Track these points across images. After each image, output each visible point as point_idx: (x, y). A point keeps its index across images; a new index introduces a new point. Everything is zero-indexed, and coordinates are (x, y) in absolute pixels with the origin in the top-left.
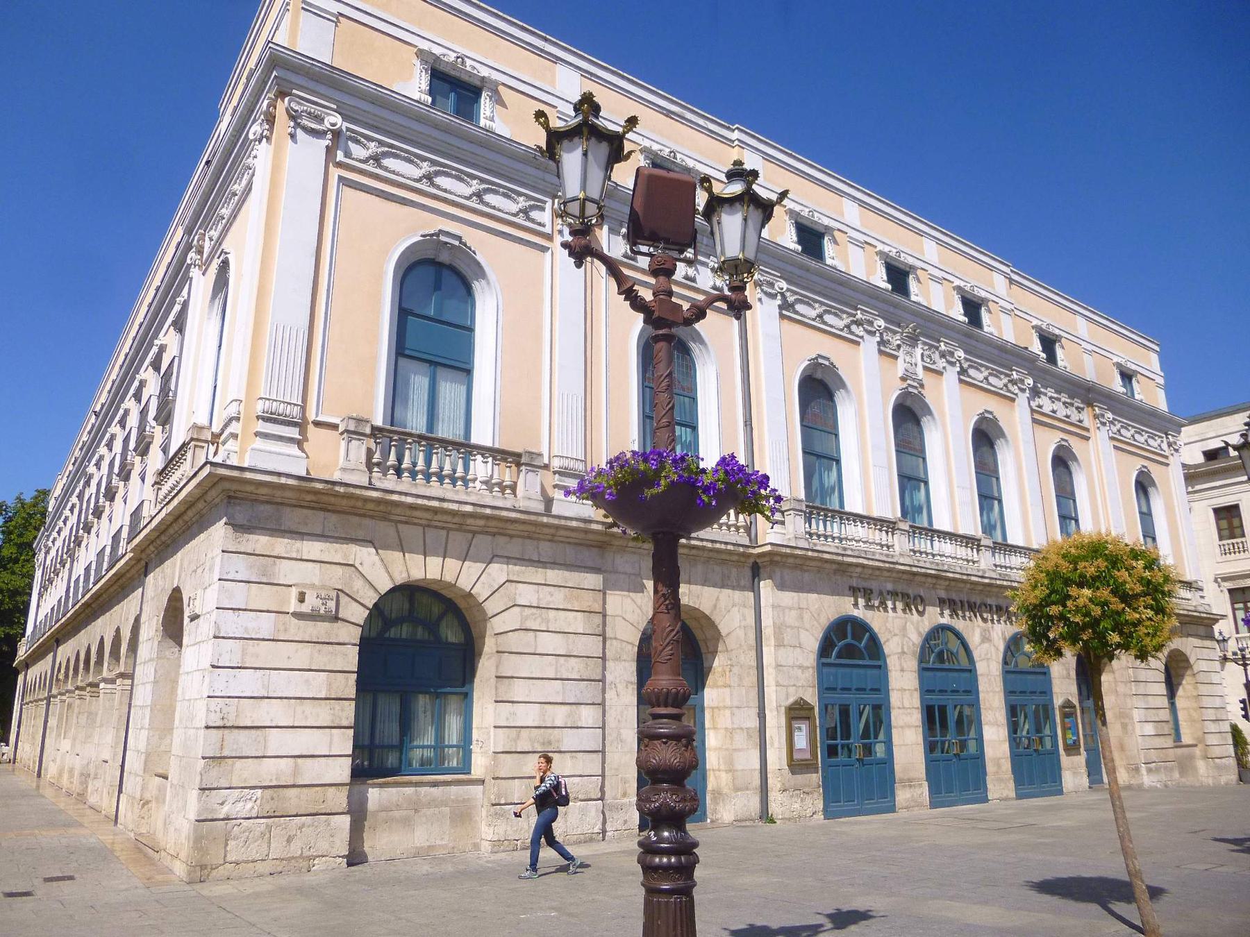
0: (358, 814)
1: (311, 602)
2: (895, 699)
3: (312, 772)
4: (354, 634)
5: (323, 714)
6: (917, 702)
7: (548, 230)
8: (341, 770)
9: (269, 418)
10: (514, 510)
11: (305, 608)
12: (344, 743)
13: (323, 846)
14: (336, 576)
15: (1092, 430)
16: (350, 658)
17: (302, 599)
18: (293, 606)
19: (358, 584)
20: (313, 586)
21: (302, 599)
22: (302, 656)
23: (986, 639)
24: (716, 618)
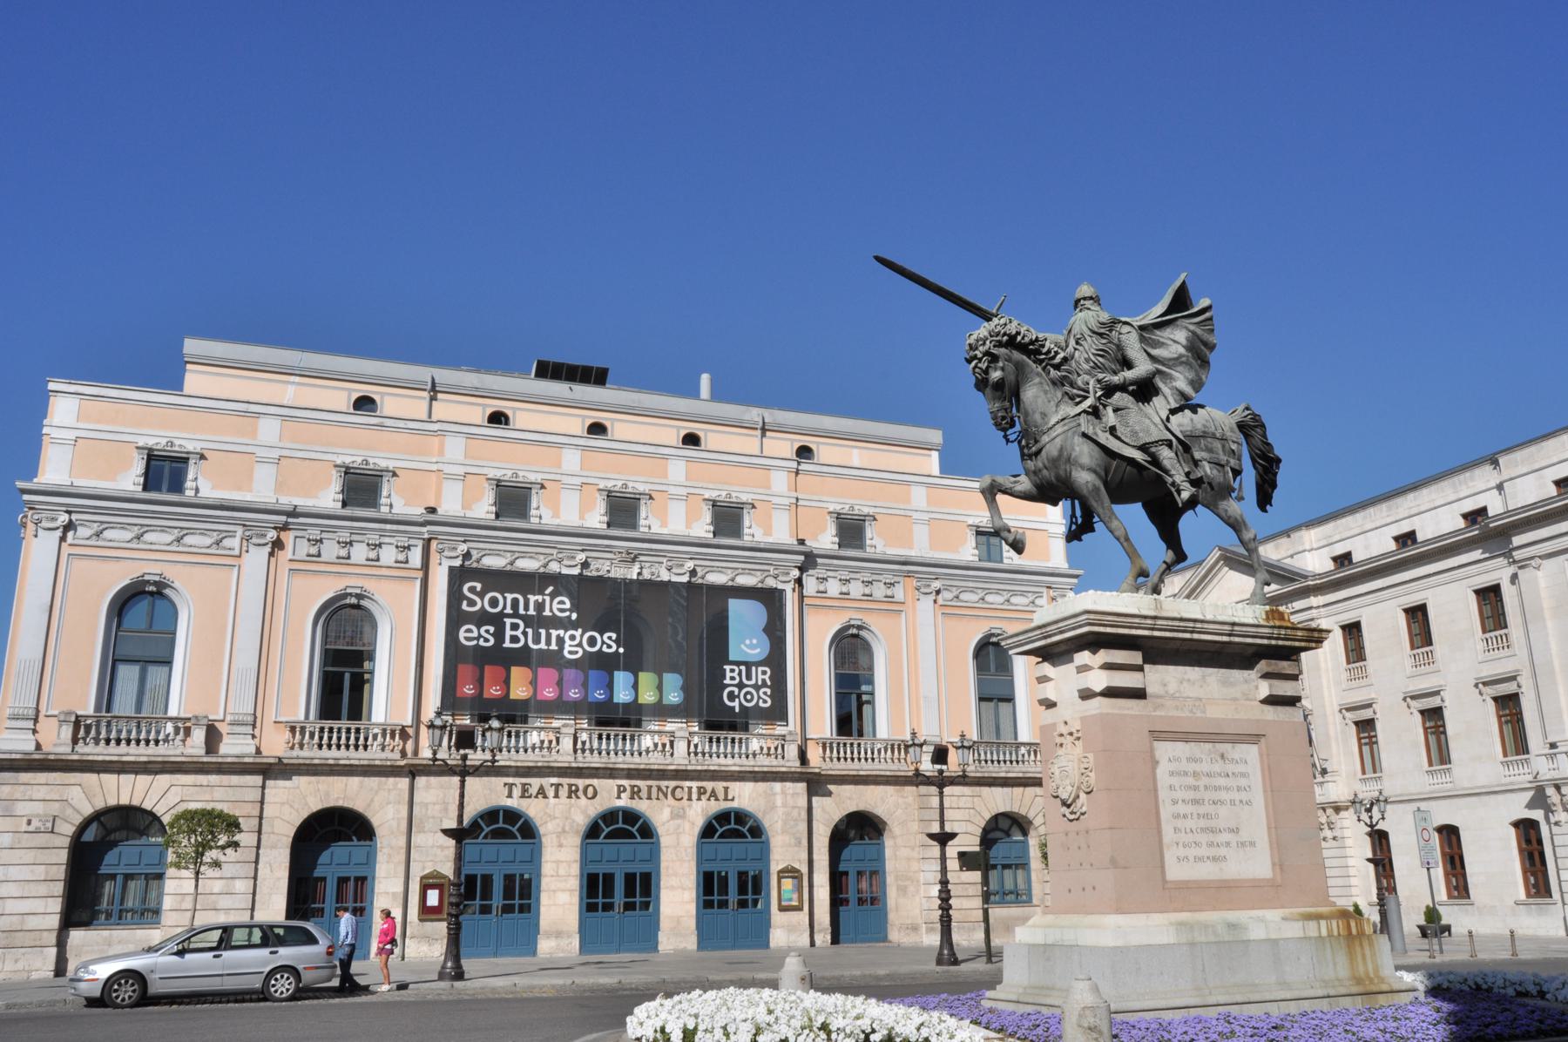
0: (61, 944)
1: (36, 824)
2: (547, 868)
3: (32, 923)
4: (66, 842)
5: (42, 889)
6: (575, 869)
7: (237, 552)
8: (54, 921)
9: (15, 718)
10: (182, 755)
11: (31, 828)
12: (56, 906)
13: (38, 964)
14: (55, 808)
15: (909, 602)
16: (63, 856)
17: (29, 822)
18: (24, 827)
19: (69, 811)
20: (37, 815)
21: (29, 822)
22: (29, 856)
23: (678, 815)
24: (369, 815)
